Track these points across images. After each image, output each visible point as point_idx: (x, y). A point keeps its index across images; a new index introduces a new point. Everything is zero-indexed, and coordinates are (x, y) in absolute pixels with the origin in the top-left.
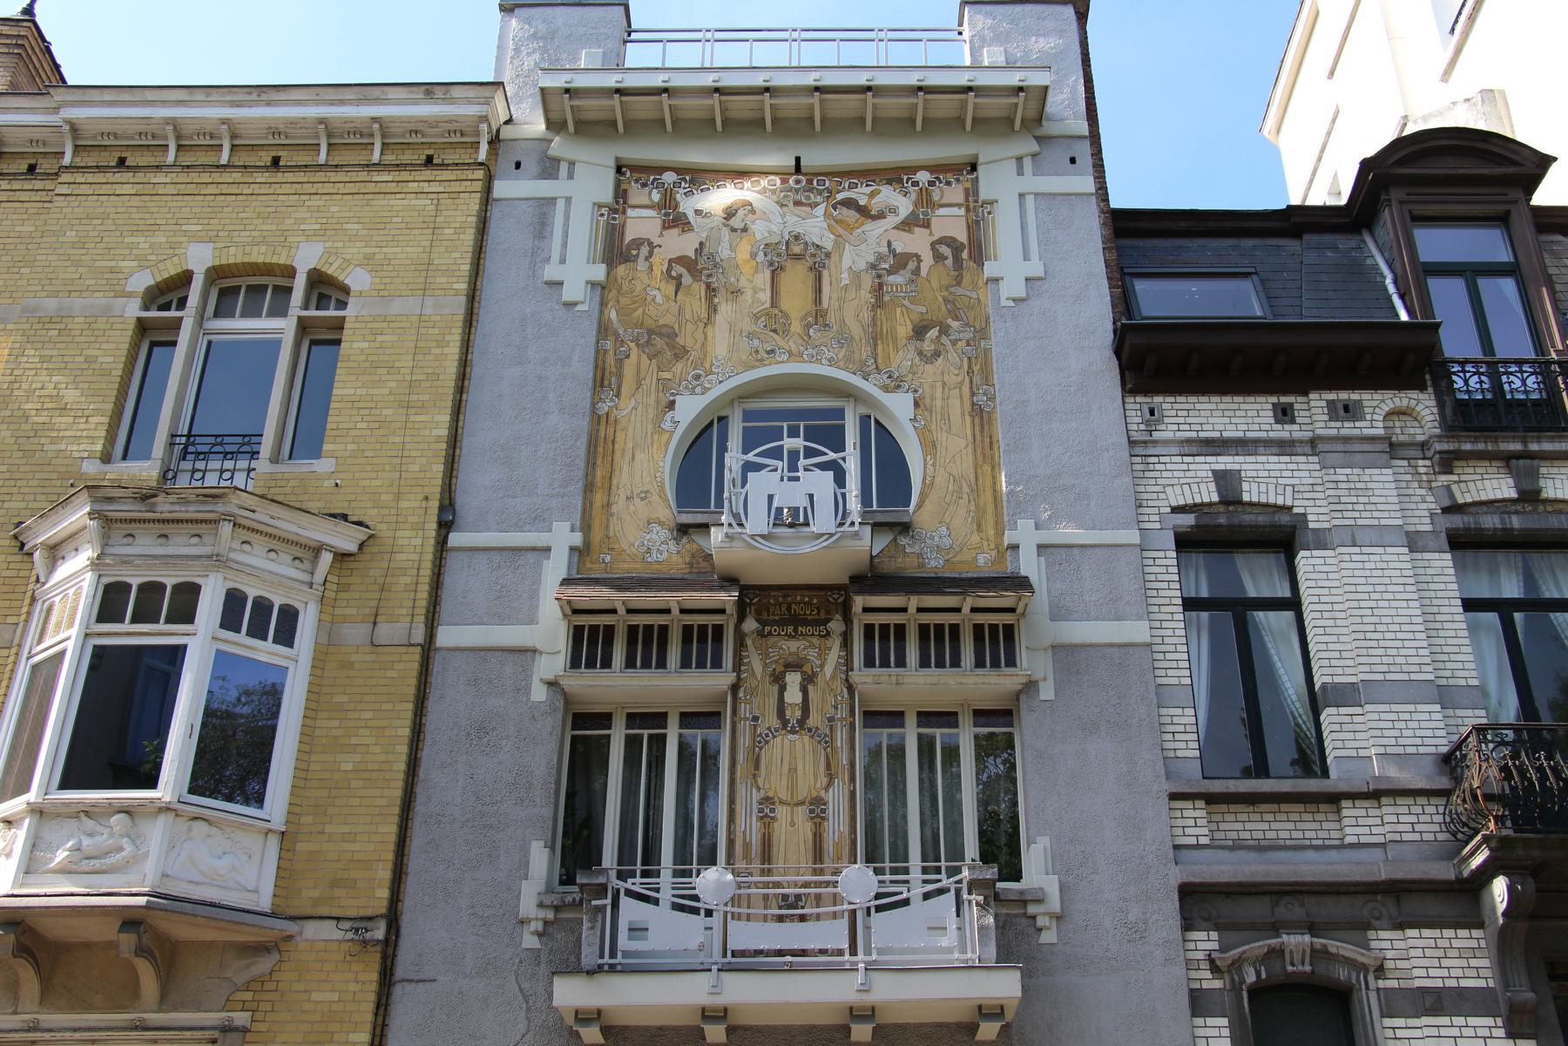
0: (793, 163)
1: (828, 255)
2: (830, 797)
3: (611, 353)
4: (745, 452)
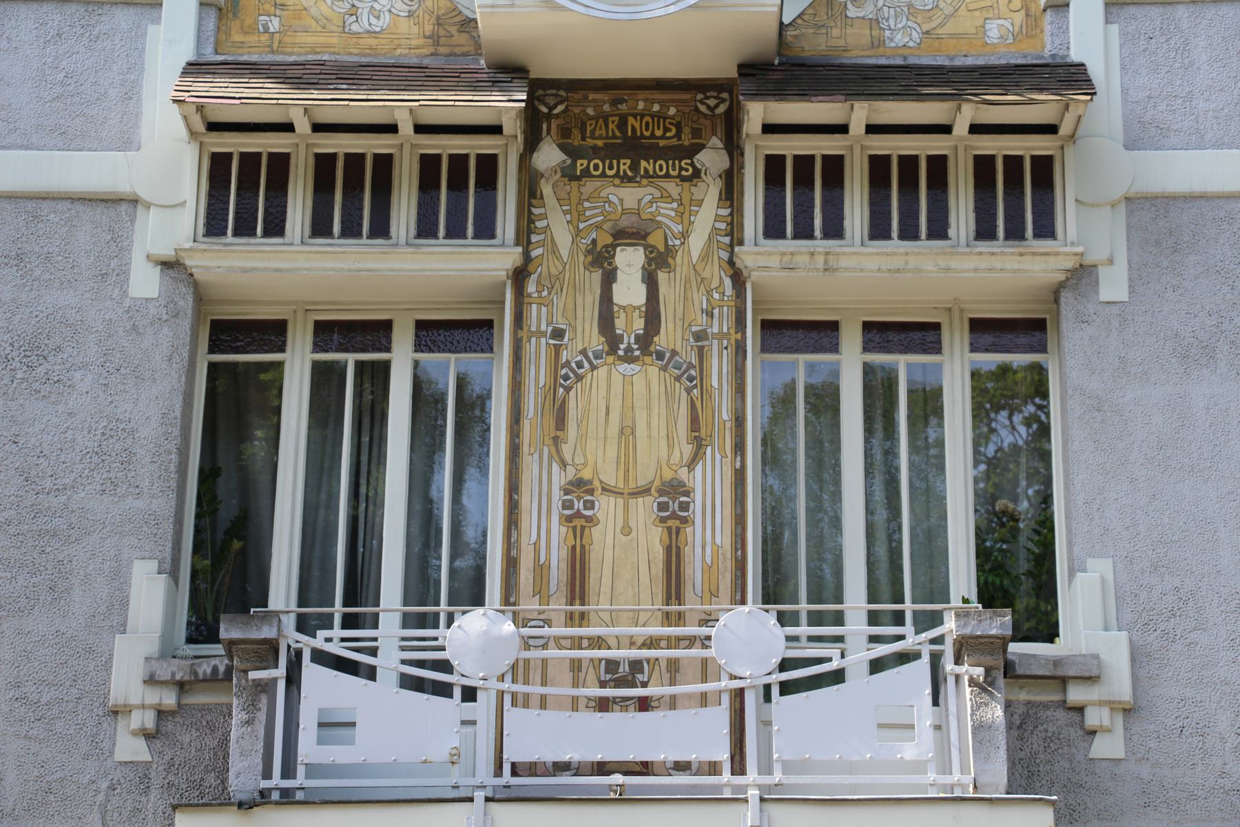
2: (696, 479)
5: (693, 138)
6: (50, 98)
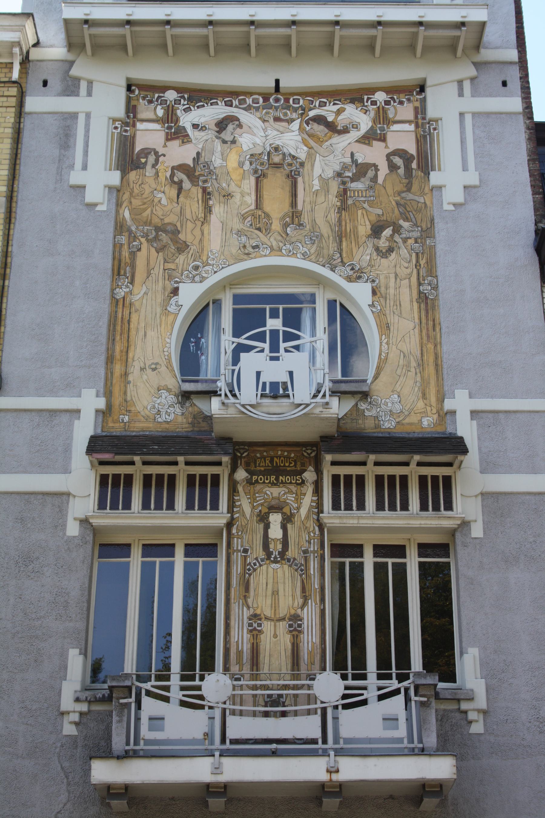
0: (273, 84)
1: (302, 164)
2: (305, 614)
3: (126, 247)
4: (237, 333)
5: (301, 467)
6: (34, 451)
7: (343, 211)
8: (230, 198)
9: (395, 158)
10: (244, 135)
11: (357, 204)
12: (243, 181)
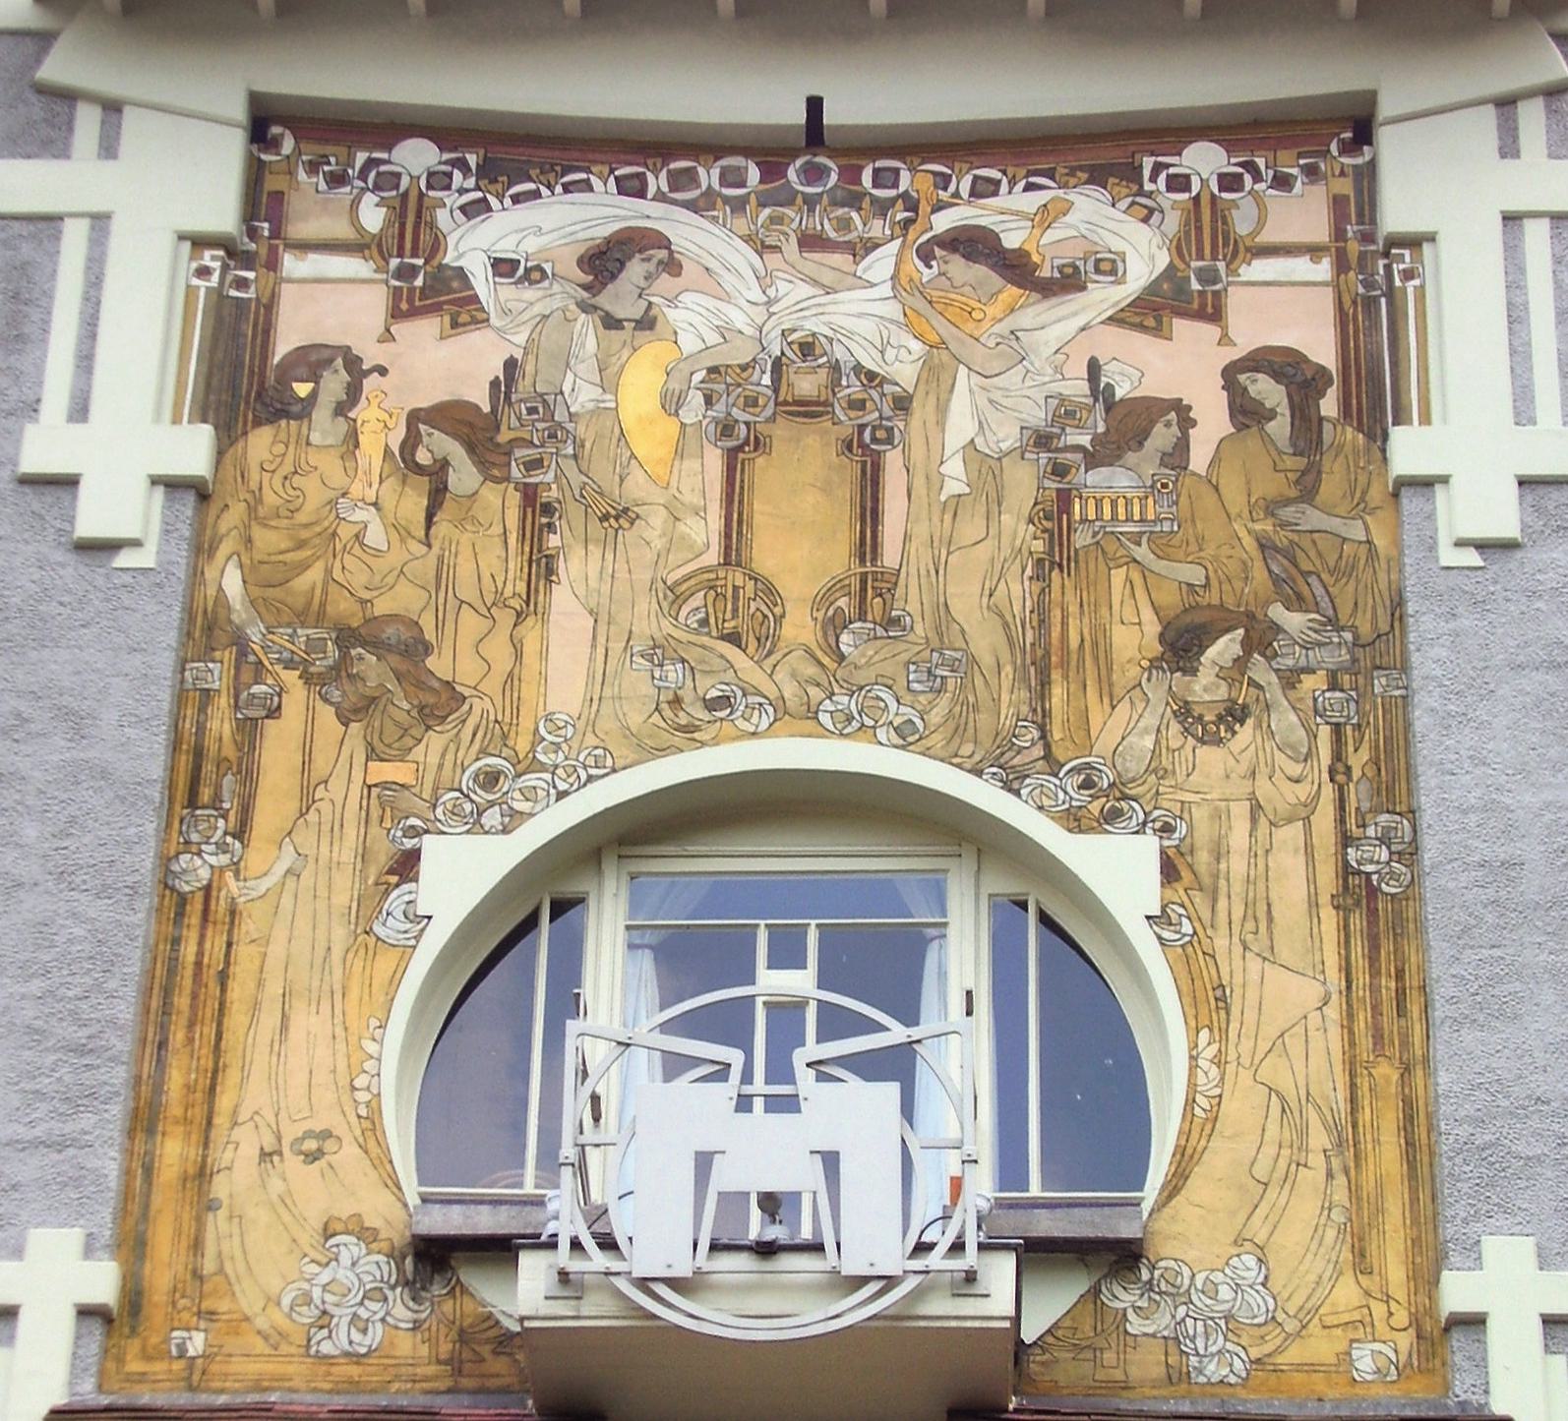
0: (800, 117)
1: (903, 404)
3: (224, 701)
7: (1055, 573)
8: (626, 525)
9: (1255, 381)
10: (686, 298)
11: (1111, 547)
12: (676, 463)
